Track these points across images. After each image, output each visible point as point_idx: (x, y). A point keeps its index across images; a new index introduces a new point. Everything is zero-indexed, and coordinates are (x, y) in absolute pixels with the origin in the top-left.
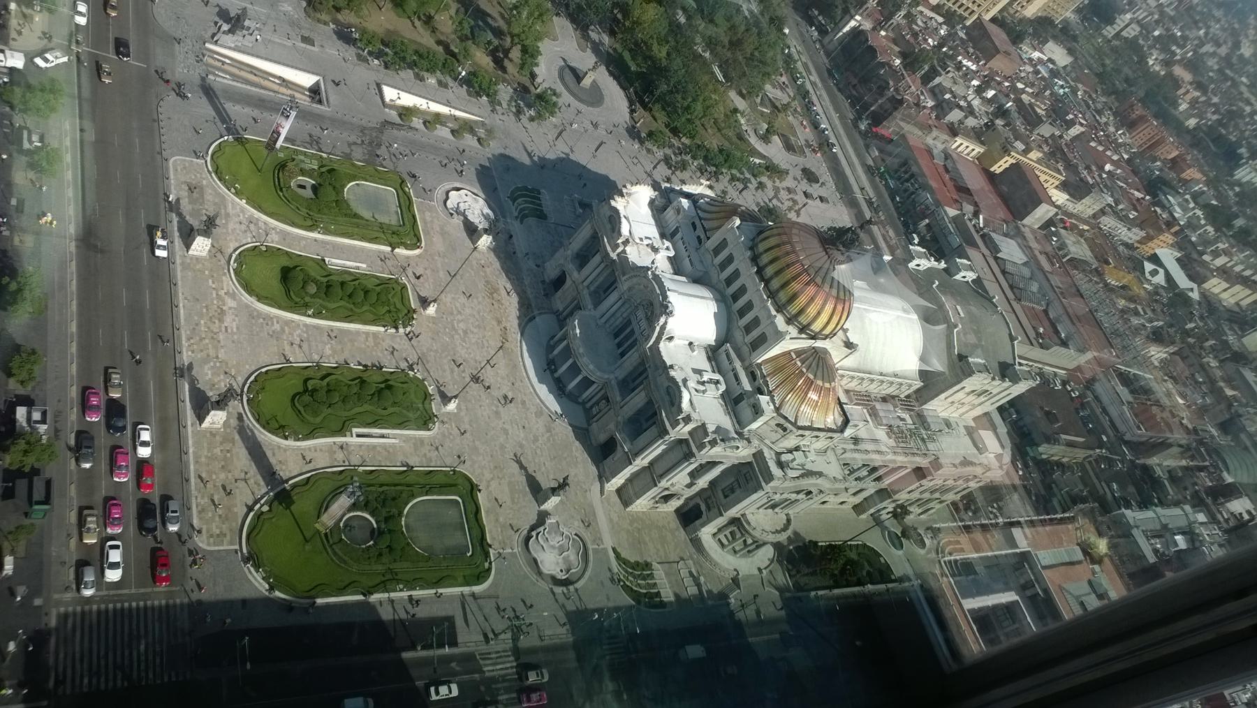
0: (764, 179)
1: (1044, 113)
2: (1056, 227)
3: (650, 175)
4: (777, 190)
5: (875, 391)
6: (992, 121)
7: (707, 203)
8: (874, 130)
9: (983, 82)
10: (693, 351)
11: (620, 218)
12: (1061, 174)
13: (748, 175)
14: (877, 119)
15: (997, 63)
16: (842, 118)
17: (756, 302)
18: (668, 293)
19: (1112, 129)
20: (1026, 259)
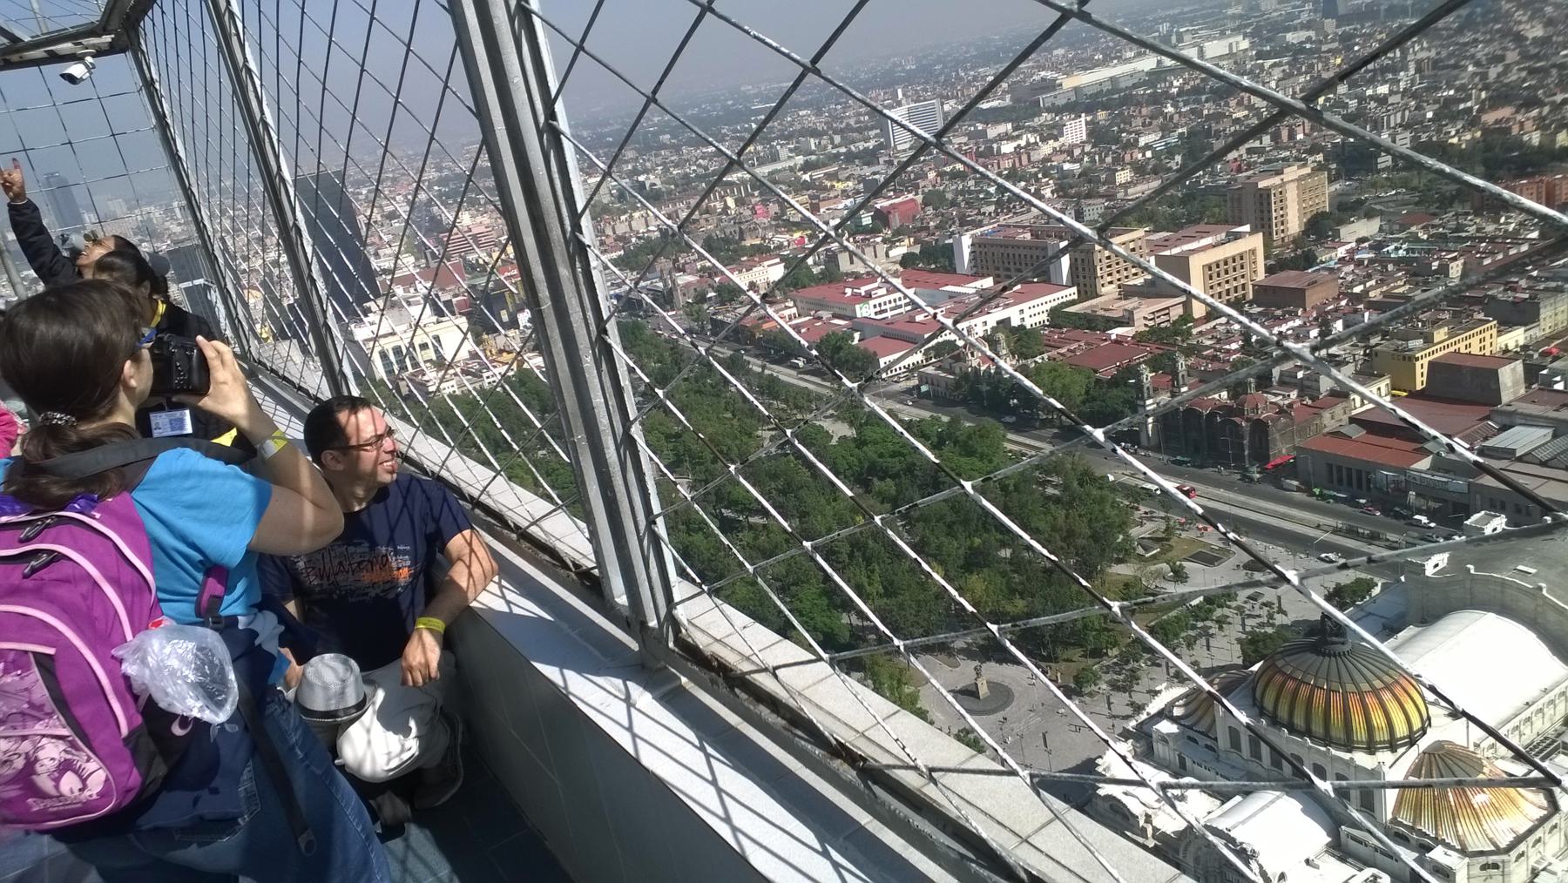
0: (1218, 612)
1: (1407, 287)
2: (1544, 368)
3: (1115, 717)
4: (1240, 609)
5: (1548, 724)
6: (1366, 347)
7: (1185, 705)
8: (1269, 466)
9: (1320, 326)
10: (1317, 867)
11: (1119, 801)
12: (1489, 321)
13: (1200, 624)
14: (1261, 454)
15: (1314, 298)
16: (1229, 486)
17: (1320, 761)
18: (1232, 834)
19: (1490, 228)
20: (1549, 432)
